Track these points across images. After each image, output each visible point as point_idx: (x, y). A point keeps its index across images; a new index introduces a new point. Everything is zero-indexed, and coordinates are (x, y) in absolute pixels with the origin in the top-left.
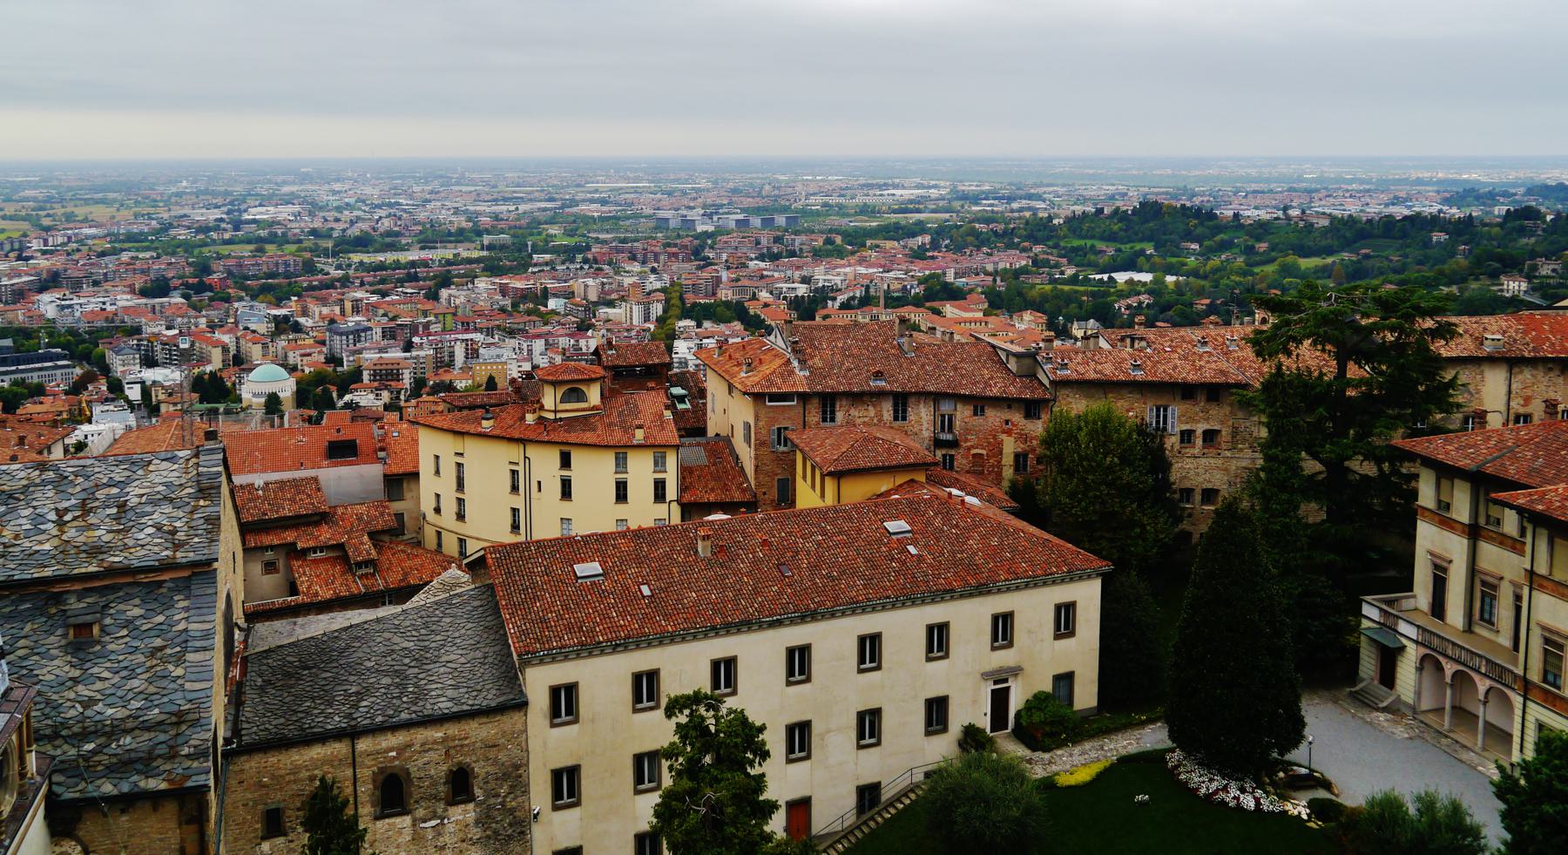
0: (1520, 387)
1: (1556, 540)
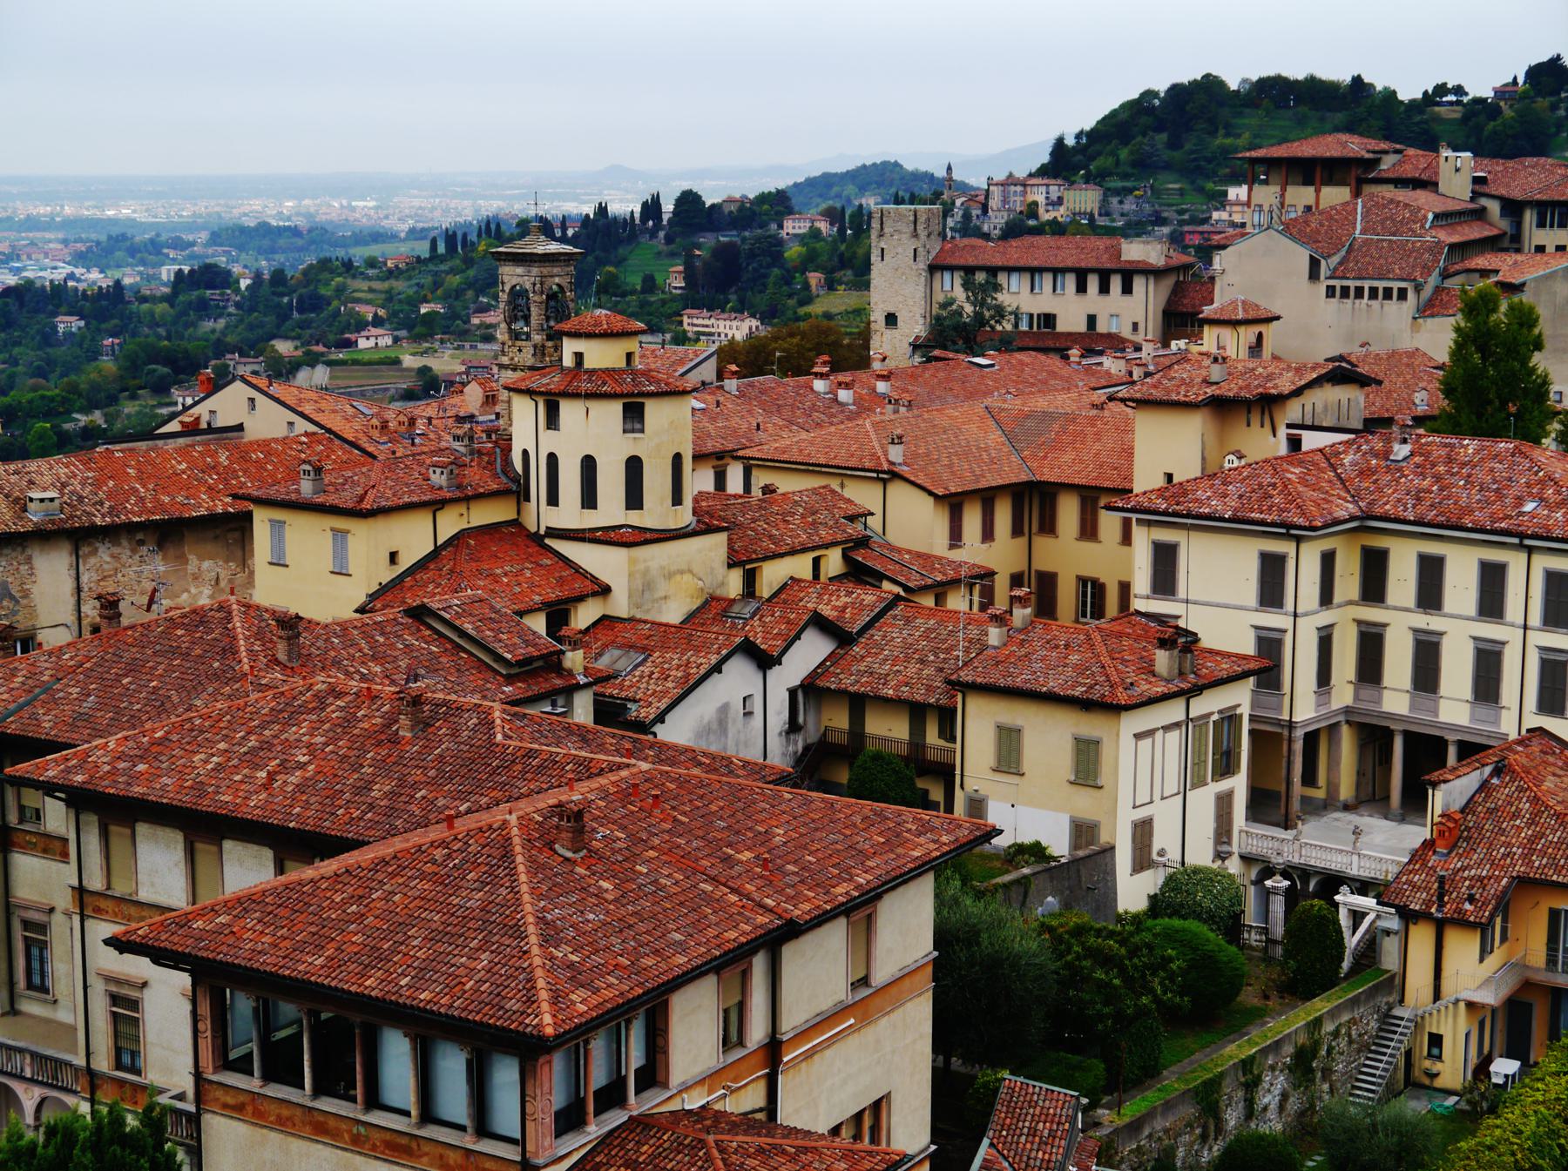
0: (95, 578)
1: (113, 829)
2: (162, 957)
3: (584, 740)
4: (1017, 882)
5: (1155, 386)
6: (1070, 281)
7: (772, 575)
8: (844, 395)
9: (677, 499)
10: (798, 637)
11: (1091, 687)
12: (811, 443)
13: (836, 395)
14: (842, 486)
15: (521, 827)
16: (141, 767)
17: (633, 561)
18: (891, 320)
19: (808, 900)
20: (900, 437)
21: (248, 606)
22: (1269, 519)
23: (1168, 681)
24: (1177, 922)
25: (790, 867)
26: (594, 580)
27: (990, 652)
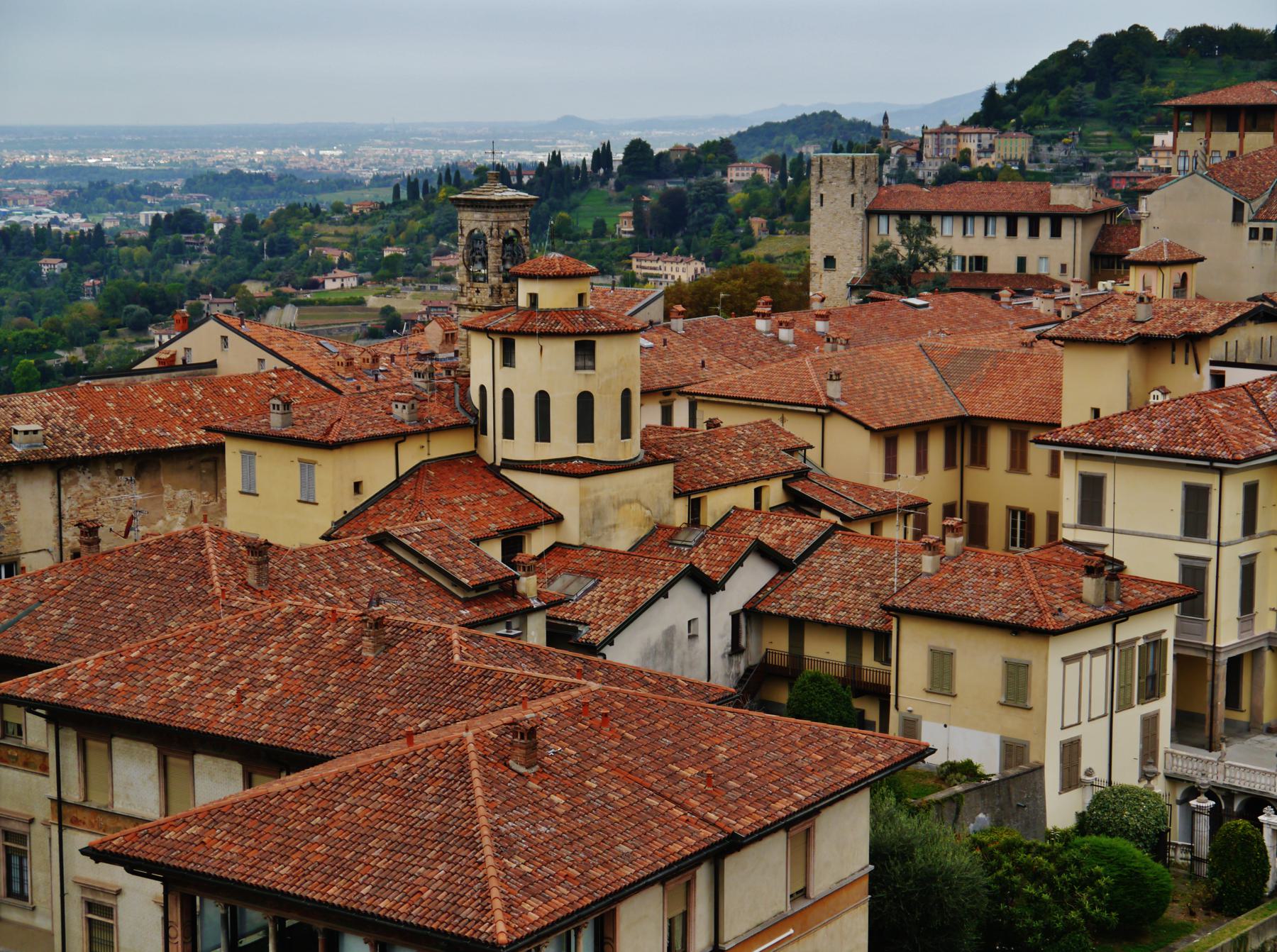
0: (76, 505)
2: (135, 866)
3: (537, 661)
4: (950, 799)
5: (1082, 325)
6: (1001, 225)
7: (716, 504)
8: (784, 334)
9: (626, 433)
10: (740, 563)
11: (1021, 613)
12: (753, 379)
13: (777, 334)
14: (783, 420)
15: (477, 742)
16: (118, 685)
17: (584, 492)
18: (830, 262)
19: (750, 815)
20: (838, 374)
21: (220, 533)
22: (1193, 452)
23: (1095, 607)
24: (1104, 840)
25: (732, 783)
26: (547, 509)
27: (923, 579)
